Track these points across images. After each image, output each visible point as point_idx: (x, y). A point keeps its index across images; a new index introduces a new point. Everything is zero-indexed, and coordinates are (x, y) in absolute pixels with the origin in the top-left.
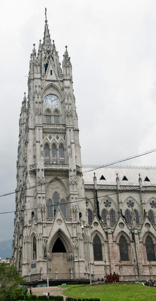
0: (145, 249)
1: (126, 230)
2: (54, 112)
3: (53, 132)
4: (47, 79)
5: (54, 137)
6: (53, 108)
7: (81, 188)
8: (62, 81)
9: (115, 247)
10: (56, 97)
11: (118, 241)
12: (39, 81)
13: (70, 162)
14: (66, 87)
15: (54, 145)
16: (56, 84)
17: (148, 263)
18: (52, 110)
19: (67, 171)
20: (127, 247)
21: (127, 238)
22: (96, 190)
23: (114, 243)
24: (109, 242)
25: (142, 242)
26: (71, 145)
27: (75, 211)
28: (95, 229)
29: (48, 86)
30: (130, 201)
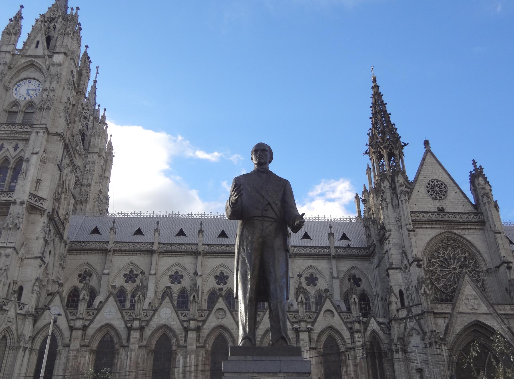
0: (151, 362)
3: (7, 138)
4: (26, 54)
6: (27, 99)
8: (51, 57)
9: (85, 357)
10: (37, 82)
11: (95, 345)
13: (18, 188)
14: (53, 64)
16: (39, 61)
18: (22, 104)
19: (7, 205)
23: (84, 349)
24: (72, 348)
25: (146, 346)
29: (24, 65)
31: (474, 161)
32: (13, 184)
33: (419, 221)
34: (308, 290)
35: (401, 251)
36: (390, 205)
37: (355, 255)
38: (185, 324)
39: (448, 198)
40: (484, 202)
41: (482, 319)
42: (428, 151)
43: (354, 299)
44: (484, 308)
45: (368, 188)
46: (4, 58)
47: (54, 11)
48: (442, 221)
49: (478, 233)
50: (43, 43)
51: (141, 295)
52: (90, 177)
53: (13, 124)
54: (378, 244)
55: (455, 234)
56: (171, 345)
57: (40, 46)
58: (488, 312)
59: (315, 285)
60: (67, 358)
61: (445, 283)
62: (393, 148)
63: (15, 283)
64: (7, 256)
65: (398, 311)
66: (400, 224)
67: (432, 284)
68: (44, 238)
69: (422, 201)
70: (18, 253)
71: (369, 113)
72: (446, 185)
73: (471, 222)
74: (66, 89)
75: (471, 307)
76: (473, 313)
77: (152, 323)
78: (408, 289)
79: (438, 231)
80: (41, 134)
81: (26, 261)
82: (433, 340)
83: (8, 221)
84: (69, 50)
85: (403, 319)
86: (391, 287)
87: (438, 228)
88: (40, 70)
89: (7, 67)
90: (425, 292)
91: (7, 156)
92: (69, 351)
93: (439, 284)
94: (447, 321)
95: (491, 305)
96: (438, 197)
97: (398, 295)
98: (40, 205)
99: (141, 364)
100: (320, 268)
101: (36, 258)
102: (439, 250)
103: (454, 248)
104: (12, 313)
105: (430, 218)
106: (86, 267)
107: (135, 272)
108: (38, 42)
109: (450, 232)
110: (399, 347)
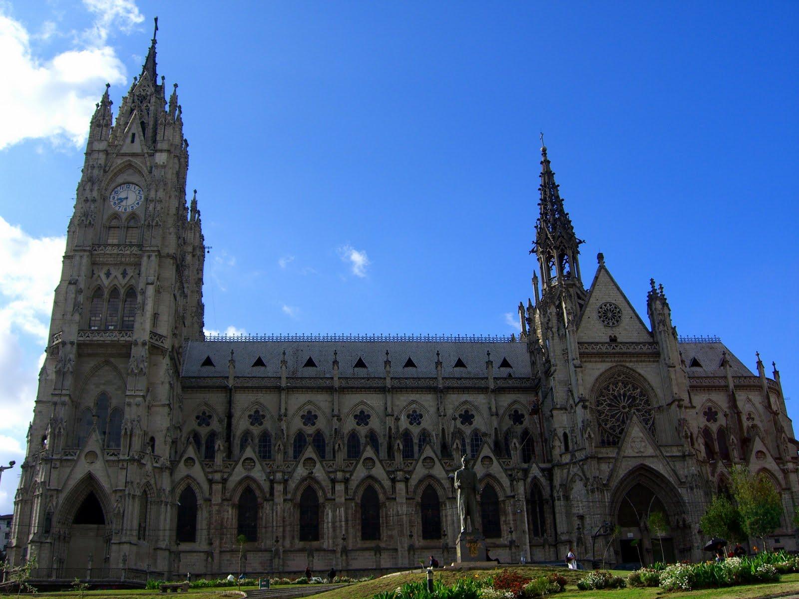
0: (297, 515)
1: (258, 473)
2: (127, 219)
4: (122, 151)
7: (163, 383)
8: (152, 155)
9: (228, 512)
10: (137, 187)
11: (236, 499)
12: (102, 156)
13: (137, 326)
14: (157, 166)
15: (114, 291)
16: (137, 161)
17: (299, 544)
18: (124, 217)
19: (129, 346)
20: (257, 512)
21: (258, 493)
22: (231, 390)
23: (226, 503)
24: (213, 502)
25: (290, 500)
26: (146, 288)
27: (129, 433)
28: (185, 474)
30: (309, 412)
31: (652, 280)
32: (126, 319)
33: (587, 354)
34: (463, 429)
35: (566, 389)
37: (516, 388)
38: (332, 476)
39: (622, 325)
40: (660, 330)
41: (648, 462)
42: (602, 268)
43: (515, 444)
44: (650, 451)
45: (534, 304)
47: (144, 86)
48: (613, 354)
49: (653, 366)
51: (281, 446)
54: (543, 377)
55: (627, 367)
56: (316, 498)
57: (137, 139)
58: (654, 454)
59: (471, 423)
60: (210, 513)
61: (613, 423)
62: (566, 248)
63: (145, 434)
64: (138, 405)
65: (561, 456)
66: (566, 358)
67: (600, 425)
68: (170, 382)
69: (594, 330)
70: (145, 401)
71: (537, 196)
72: (620, 310)
73: (645, 354)
74: (173, 197)
75: (637, 451)
76: (639, 457)
77: (295, 475)
78: (572, 431)
79: (609, 365)
80: (153, 258)
81: (154, 409)
82: (595, 486)
83: (132, 366)
84: (172, 145)
85: (567, 464)
86: (555, 430)
87: (608, 362)
88: (140, 171)
89: (102, 171)
90: (590, 436)
91: (115, 285)
92: (210, 506)
93: (606, 425)
94: (611, 466)
95: (658, 446)
96: (611, 324)
97: (562, 438)
98: (161, 344)
99: (287, 519)
100: (476, 404)
101: (164, 405)
102: (608, 386)
104: (149, 467)
105: (600, 350)
106: (205, 408)
107: (261, 413)
109: (621, 366)
110: (561, 494)
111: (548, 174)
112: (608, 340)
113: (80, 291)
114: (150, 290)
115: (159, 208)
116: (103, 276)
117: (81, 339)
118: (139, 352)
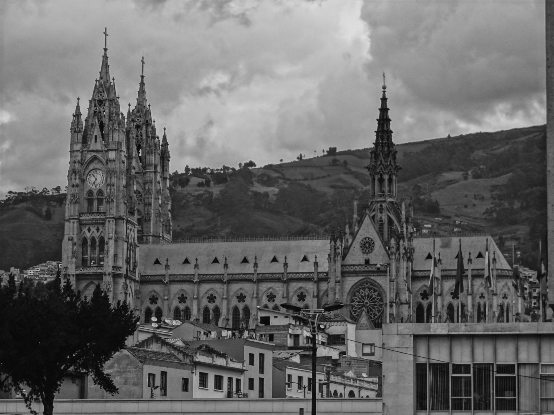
4: (91, 149)
5: (93, 229)
12: (79, 154)
14: (110, 161)
15: (93, 239)
16: (99, 155)
18: (95, 192)
30: (212, 295)
32: (101, 256)
36: (332, 260)
46: (77, 156)
50: (99, 139)
52: (150, 196)
53: (93, 213)
57: (98, 140)
59: (304, 300)
67: (351, 313)
79: (361, 278)
80: (111, 222)
98: (119, 272)
100: (307, 288)
103: (370, 289)
106: (153, 293)
108: (96, 136)
111: (384, 110)
112: (363, 262)
113: (74, 244)
114: (111, 243)
115: (112, 190)
116: (87, 232)
117: (77, 272)
118: (108, 279)
